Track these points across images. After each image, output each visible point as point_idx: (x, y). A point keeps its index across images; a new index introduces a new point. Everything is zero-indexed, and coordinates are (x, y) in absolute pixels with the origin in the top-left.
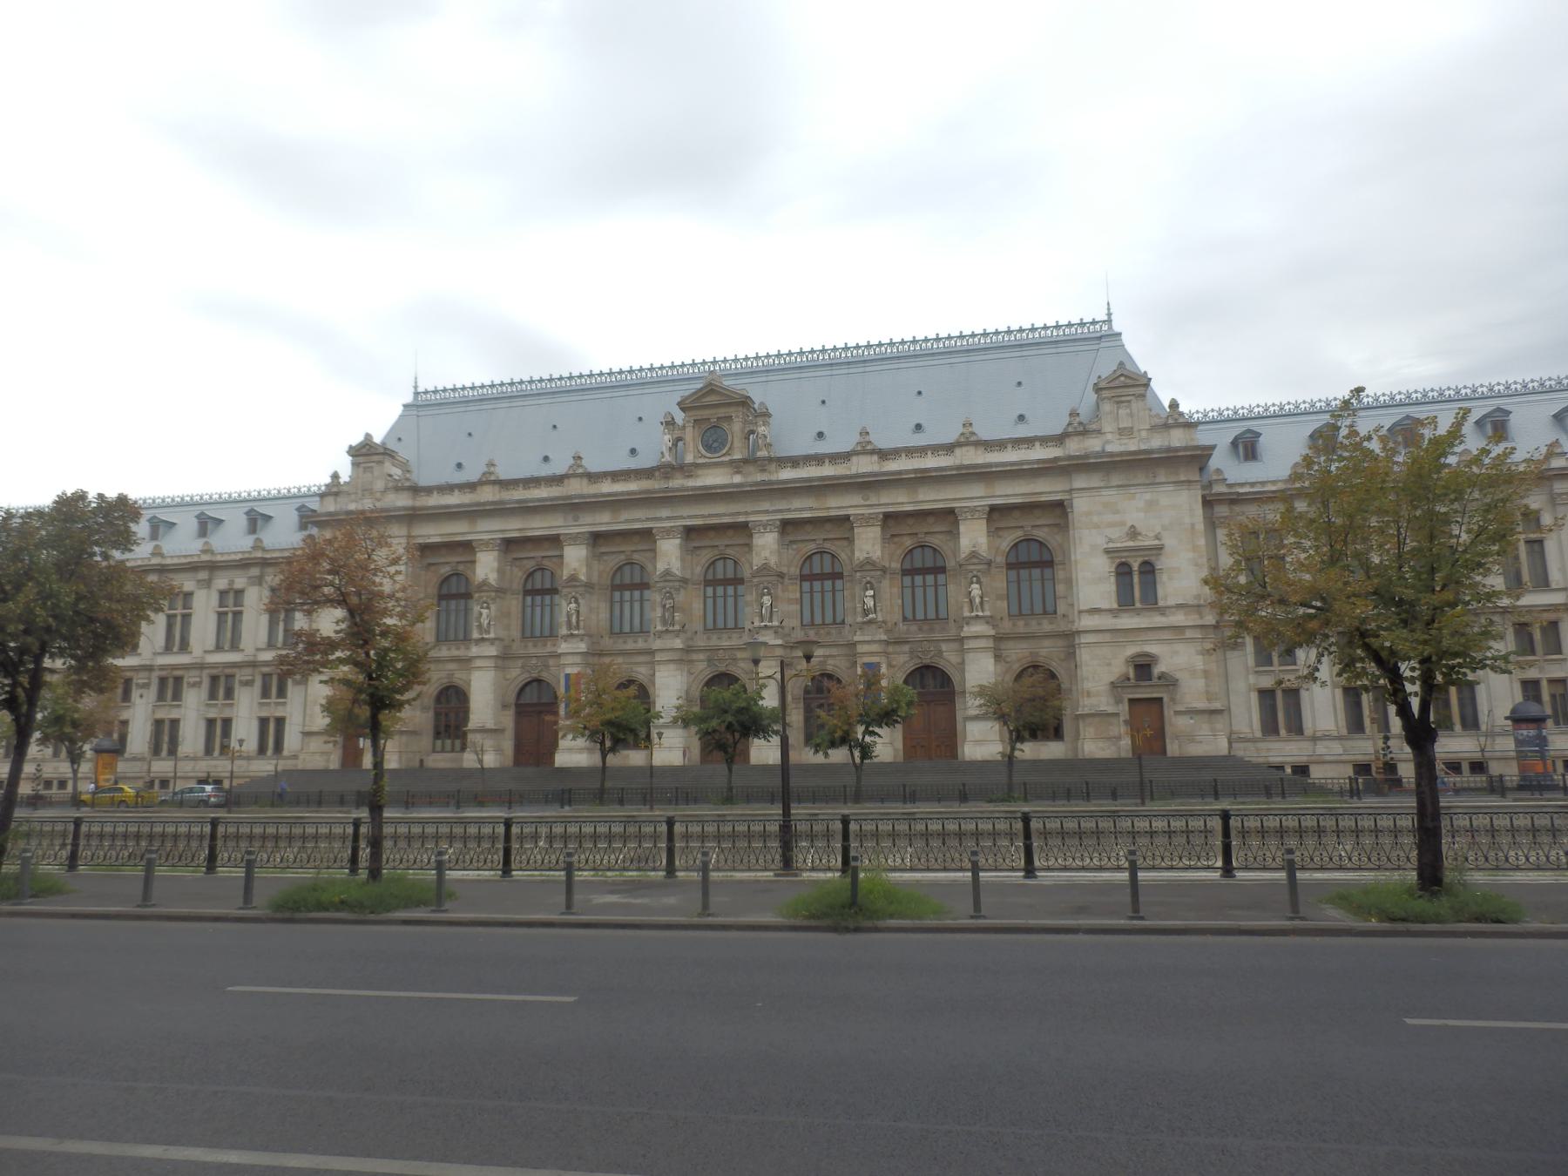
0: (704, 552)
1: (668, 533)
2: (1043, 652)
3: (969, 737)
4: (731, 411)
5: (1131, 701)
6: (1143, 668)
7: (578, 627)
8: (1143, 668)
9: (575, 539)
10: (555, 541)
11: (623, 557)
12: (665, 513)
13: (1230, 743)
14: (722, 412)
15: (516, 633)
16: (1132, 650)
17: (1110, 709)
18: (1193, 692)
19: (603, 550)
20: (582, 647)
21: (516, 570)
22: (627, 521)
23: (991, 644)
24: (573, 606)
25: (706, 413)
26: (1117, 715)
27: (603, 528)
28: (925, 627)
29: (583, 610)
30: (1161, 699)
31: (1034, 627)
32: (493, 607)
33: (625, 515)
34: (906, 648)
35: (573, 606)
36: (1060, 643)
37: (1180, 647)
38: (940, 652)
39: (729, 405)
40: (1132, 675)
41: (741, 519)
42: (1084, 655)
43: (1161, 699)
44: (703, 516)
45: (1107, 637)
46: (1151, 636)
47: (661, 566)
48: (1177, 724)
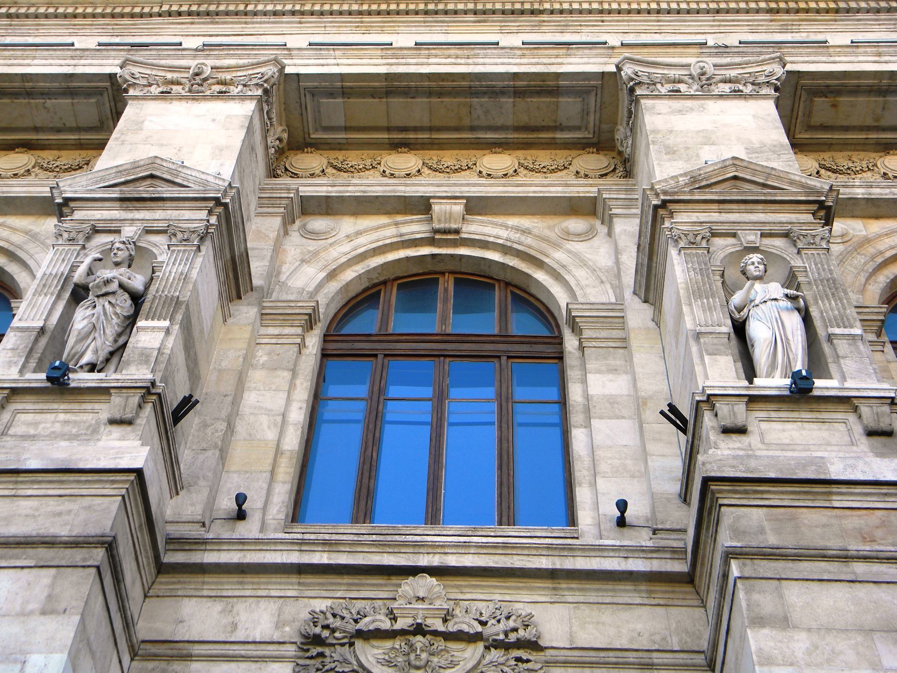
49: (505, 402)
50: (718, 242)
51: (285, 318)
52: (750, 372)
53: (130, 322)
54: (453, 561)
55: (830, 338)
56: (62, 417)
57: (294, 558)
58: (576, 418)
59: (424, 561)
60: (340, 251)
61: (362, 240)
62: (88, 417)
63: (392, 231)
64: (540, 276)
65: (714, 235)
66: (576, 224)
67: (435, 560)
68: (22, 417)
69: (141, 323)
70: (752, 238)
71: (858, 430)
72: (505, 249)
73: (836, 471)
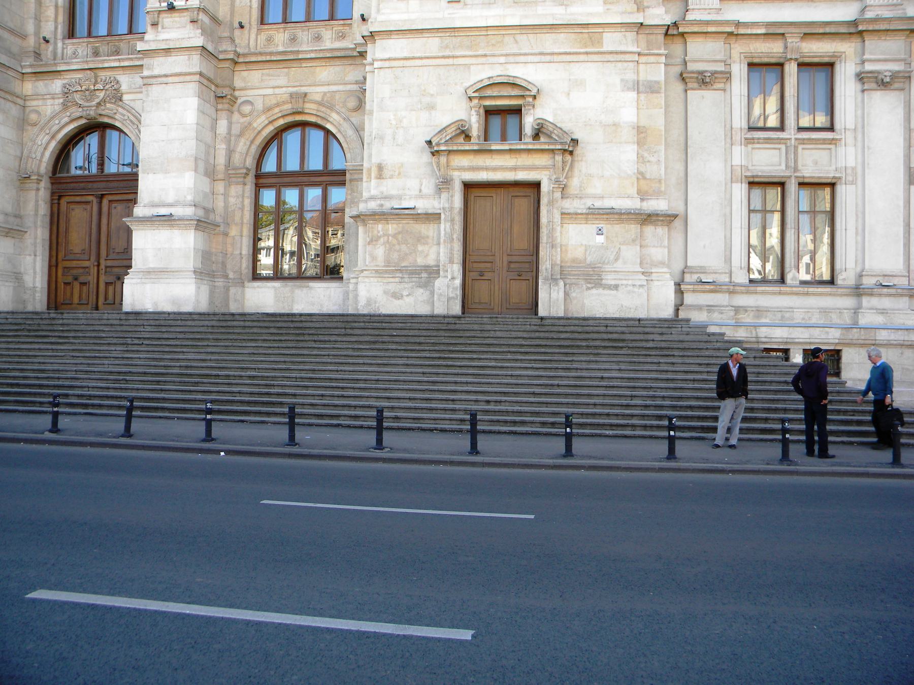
2: (316, 93)
3: (138, 259)
5: (468, 186)
6: (503, 113)
8: (503, 113)
13: (679, 291)
16: (482, 73)
17: (423, 205)
18: (607, 172)
23: (195, 63)
26: (433, 217)
28: (103, 48)
30: (537, 185)
31: (305, 42)
34: (57, 85)
36: (352, 74)
37: (588, 71)
38: (118, 97)
40: (476, 130)
42: (379, 87)
43: (537, 185)
45: (432, 45)
46: (527, 42)
48: (568, 239)
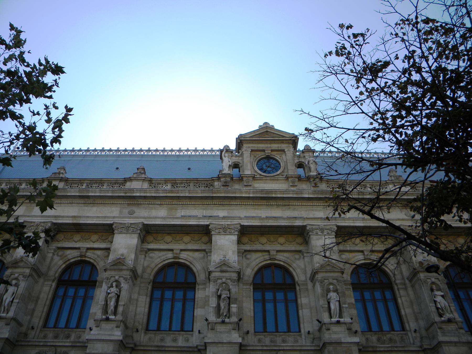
0: (254, 256)
1: (225, 230)
4: (283, 146)
7: (115, 313)
9: (127, 229)
10: (107, 230)
11: (170, 255)
12: (222, 213)
14: (275, 146)
15: (37, 321)
19: (151, 246)
20: (118, 335)
21: (56, 258)
22: (183, 217)
24: (114, 290)
25: (261, 146)
27: (158, 222)
29: (124, 294)
32: (22, 285)
33: (182, 212)
35: (114, 290)
39: (282, 142)
41: (298, 223)
44: (260, 218)
47: (216, 258)
49: (286, 296)
50: (326, 281)
51: (247, 284)
52: (331, 317)
53: (229, 304)
54: (285, 348)
55: (343, 307)
56: (224, 327)
57: (261, 348)
58: (300, 308)
59: (281, 348)
60: (254, 264)
61: (257, 260)
62: (228, 327)
63: (262, 258)
64: (291, 269)
65: (325, 279)
66: (297, 256)
67: (282, 348)
68: (218, 327)
69: (232, 306)
70: (331, 281)
71: (346, 328)
72: (284, 262)
73: (343, 340)
